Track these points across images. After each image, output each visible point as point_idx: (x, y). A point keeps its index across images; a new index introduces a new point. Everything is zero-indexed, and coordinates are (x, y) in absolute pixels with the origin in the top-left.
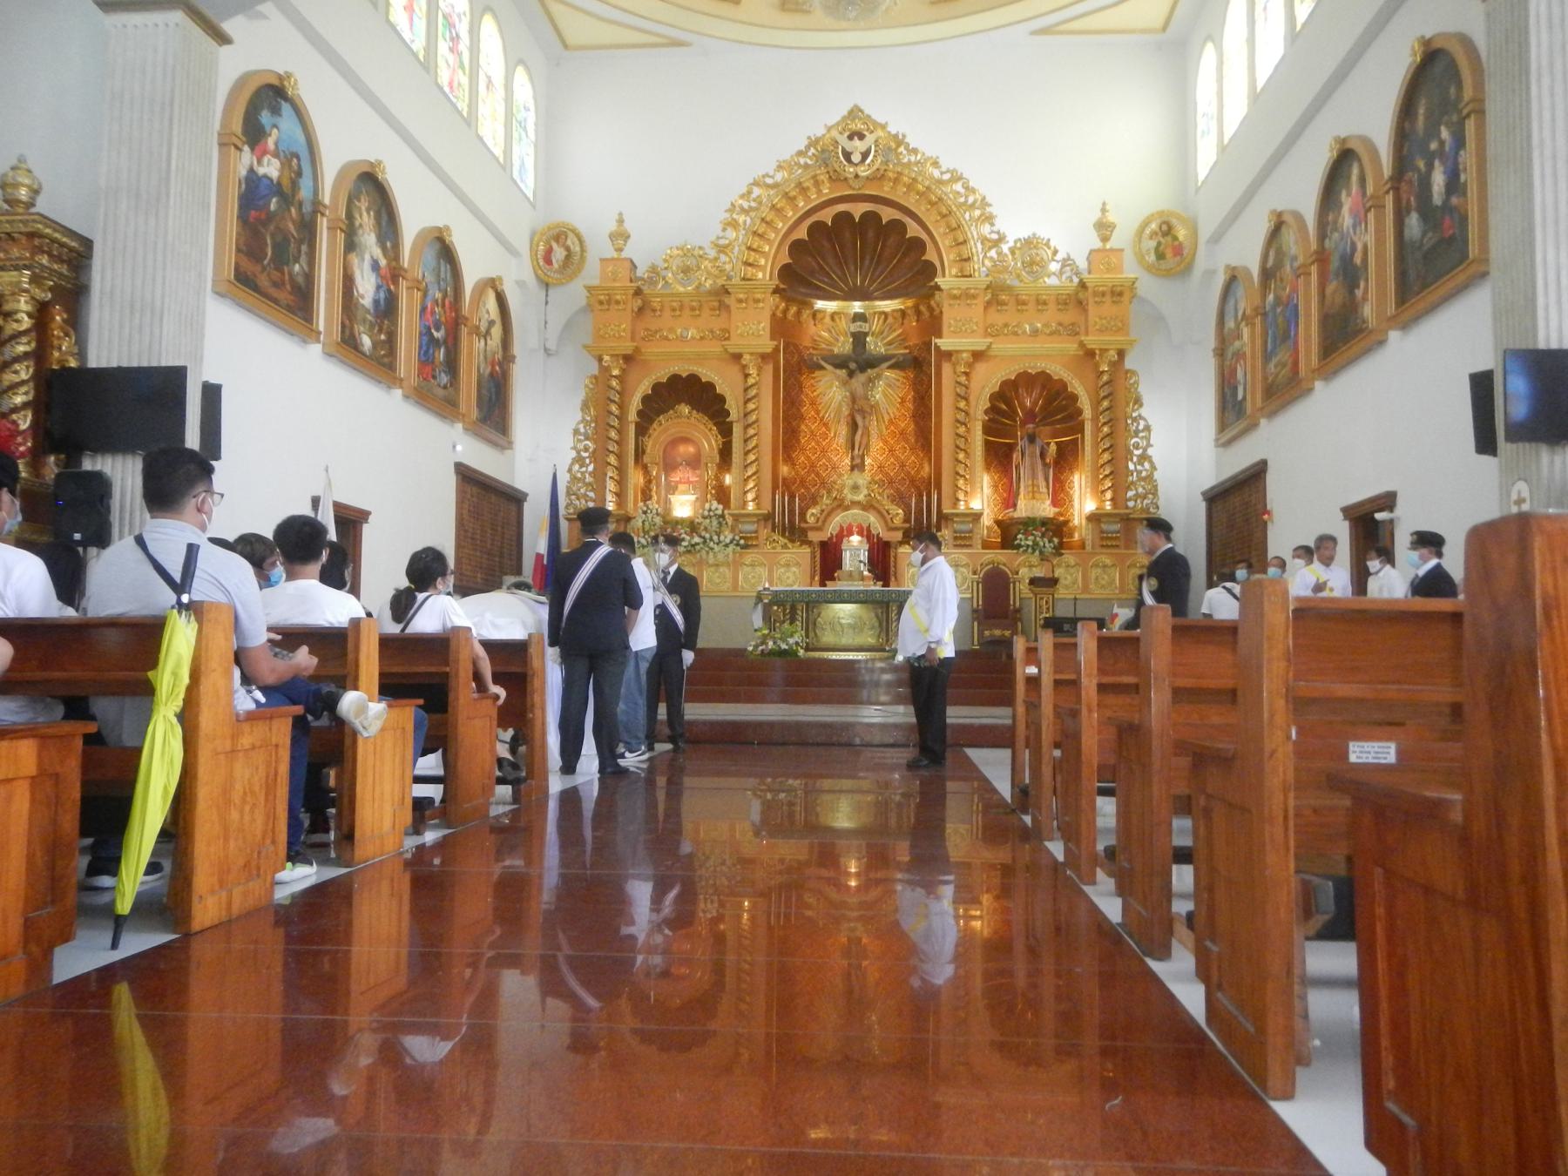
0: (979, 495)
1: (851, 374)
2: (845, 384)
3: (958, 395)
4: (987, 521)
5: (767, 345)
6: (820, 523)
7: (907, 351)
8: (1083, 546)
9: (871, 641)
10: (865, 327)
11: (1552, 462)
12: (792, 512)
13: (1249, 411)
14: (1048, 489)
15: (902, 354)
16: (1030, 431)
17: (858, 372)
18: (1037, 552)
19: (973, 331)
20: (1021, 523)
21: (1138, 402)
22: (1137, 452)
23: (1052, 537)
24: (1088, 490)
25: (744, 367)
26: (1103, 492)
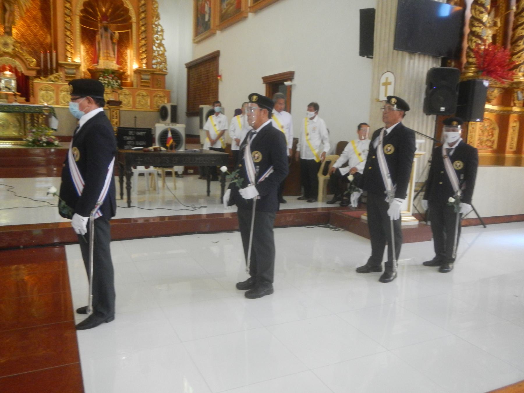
4: (83, 68)
9: (15, 134)
11: (409, 63)
13: (212, 26)
16: (105, 25)
18: (110, 87)
20: (102, 72)
21: (158, 17)
23: (117, 79)
26: (142, 59)
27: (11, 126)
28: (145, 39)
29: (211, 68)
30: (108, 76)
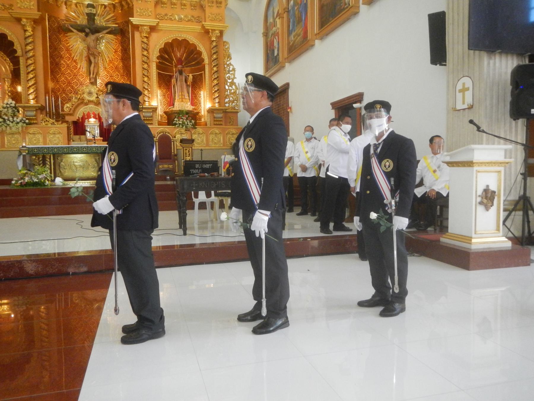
0: (155, 99)
1: (87, 35)
2: (84, 40)
3: (143, 48)
4: (160, 112)
5: (36, 14)
6: (72, 110)
7: (117, 25)
8: (206, 125)
10: (94, 11)
11: (489, 64)
12: (57, 107)
13: (280, 60)
14: (189, 98)
15: (114, 27)
17: (90, 34)
18: (184, 127)
19: (149, 16)
20: (176, 113)
21: (229, 57)
22: (229, 81)
23: (191, 120)
24: (208, 98)
25: (24, 26)
26: (214, 99)
27: (90, 167)
28: (217, 79)
29: (282, 102)
30: (182, 116)
